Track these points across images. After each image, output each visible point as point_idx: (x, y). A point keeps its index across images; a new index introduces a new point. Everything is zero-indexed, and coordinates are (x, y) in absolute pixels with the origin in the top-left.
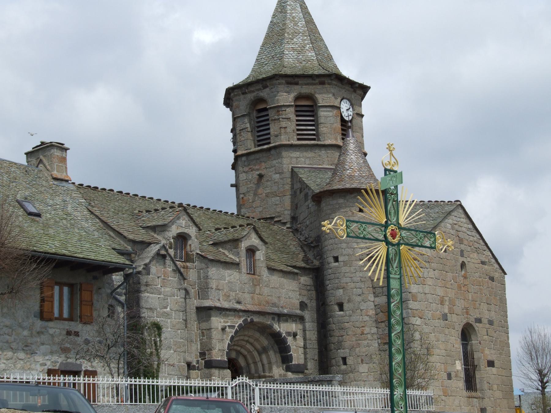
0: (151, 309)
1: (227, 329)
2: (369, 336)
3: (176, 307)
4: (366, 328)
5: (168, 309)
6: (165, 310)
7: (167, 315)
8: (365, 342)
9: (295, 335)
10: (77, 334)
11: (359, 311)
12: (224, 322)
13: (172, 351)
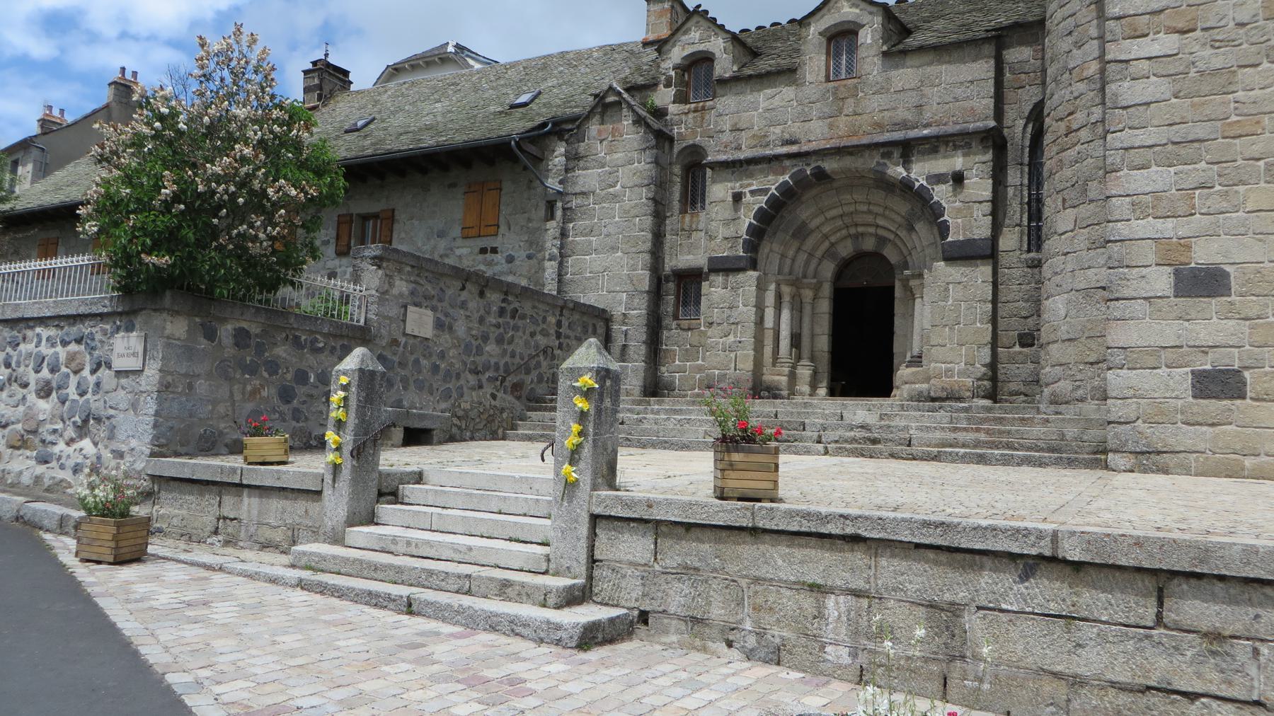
0: (583, 193)
1: (748, 198)
2: (1084, 134)
3: (637, 180)
4: (1078, 115)
5: (618, 187)
6: (611, 190)
7: (615, 196)
8: (1072, 153)
9: (958, 179)
10: (494, 250)
11: (1067, 75)
12: (741, 186)
13: (620, 254)
